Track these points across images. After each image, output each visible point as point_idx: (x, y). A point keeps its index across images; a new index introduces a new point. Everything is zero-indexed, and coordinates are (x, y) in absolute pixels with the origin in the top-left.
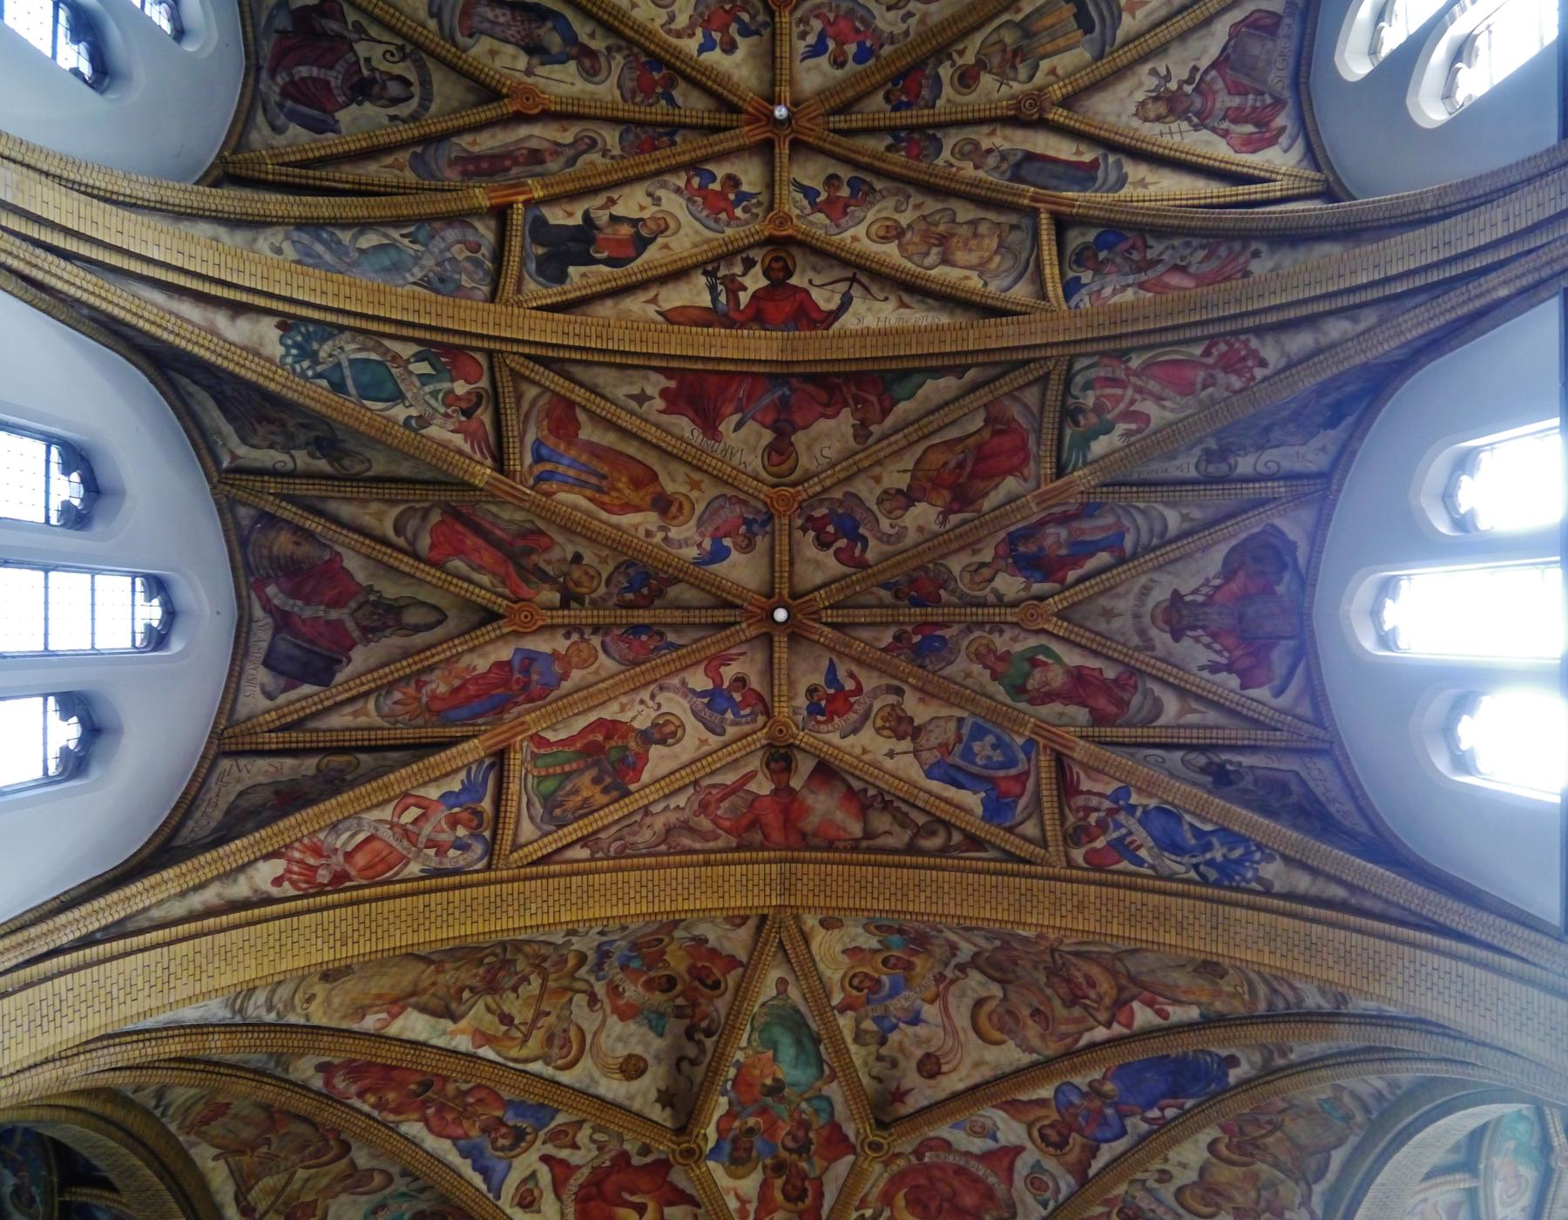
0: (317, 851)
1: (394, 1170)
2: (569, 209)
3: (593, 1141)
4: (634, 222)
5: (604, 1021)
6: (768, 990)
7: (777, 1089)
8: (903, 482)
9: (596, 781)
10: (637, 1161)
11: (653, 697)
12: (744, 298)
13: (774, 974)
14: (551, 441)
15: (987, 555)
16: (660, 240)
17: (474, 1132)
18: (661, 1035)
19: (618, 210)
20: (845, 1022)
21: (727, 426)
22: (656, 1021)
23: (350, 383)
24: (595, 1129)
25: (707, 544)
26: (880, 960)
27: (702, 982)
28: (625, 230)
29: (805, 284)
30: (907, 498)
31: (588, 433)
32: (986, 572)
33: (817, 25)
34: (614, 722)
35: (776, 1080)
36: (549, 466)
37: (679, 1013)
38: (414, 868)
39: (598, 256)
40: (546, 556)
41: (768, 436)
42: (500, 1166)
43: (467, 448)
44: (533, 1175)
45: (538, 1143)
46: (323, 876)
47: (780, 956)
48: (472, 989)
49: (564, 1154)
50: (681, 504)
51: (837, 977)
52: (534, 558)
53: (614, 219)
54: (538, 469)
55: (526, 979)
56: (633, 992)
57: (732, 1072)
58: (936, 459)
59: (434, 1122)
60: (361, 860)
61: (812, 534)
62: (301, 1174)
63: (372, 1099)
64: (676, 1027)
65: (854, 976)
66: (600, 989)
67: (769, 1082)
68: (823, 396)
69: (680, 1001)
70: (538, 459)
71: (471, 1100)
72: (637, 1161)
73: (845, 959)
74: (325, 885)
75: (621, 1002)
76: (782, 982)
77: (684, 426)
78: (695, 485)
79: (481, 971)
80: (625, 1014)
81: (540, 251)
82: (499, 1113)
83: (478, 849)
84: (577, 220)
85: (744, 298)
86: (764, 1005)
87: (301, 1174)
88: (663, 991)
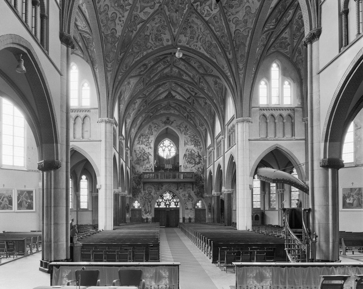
1: (231, 22)
3: (204, 10)
5: (200, 25)
6: (177, 30)
7: (177, 11)
8: (159, 68)
10: (199, 3)
13: (176, 33)
14: (195, 75)
15: (149, 65)
17: (219, 22)
18: (192, 20)
20: (165, 24)
21: (177, 71)
22: (193, 21)
24: (203, 14)
26: (161, 32)
27: (186, 28)
30: (158, 67)
31: (191, 75)
32: (149, 63)
33: (167, 87)
35: (176, 13)
37: (189, 23)
40: (198, 64)
41: (173, 69)
42: (218, 14)
44: (214, 9)
45: (212, 14)
47: (175, 36)
48: (213, 46)
49: (209, 10)
51: (167, 31)
52: (199, 64)
55: (207, 41)
56: (195, 27)
57: (183, 17)
58: (155, 71)
59: (224, 29)
61: (169, 61)
62: (242, 30)
63: (228, 41)
64: (190, 21)
65: (165, 29)
66: (199, 31)
67: (177, 13)
68: (167, 74)
69: (189, 24)
71: (218, 29)
72: (199, 3)
73: (166, 33)
75: (197, 26)
76: (175, 32)
77: (182, 73)
78: (181, 67)
79: (211, 49)
80: (197, 24)
82: (216, 24)
86: (177, 28)
87: (242, 30)
88: (191, 26)
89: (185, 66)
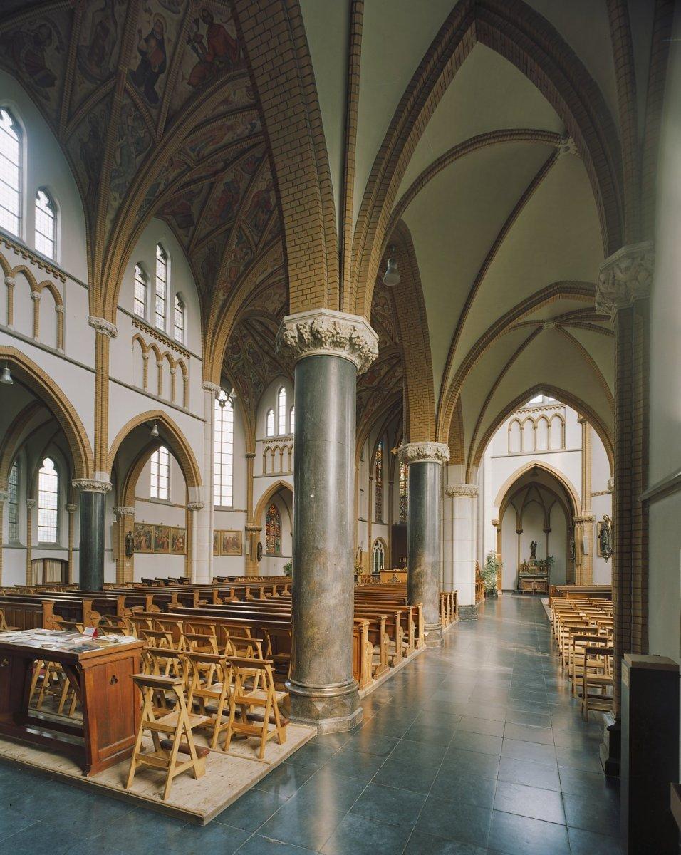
0: (224, 282)
2: (133, 56)
4: (152, 35)
9: (263, 212)
11: (262, 178)
12: (205, 42)
16: (165, 38)
19: (144, 36)
23: (151, 198)
25: (249, 126)
28: (153, 43)
29: (220, 23)
34: (258, 192)
36: (198, 148)
38: (242, 268)
39: (156, 71)
43: (179, 170)
46: (229, 286)
50: (235, 124)
53: (147, 40)
54: (196, 153)
60: (232, 276)
70: (193, 150)
74: (232, 289)
81: (143, 89)
83: (249, 251)
84: (140, 57)
85: (205, 42)
89: (230, 128)
